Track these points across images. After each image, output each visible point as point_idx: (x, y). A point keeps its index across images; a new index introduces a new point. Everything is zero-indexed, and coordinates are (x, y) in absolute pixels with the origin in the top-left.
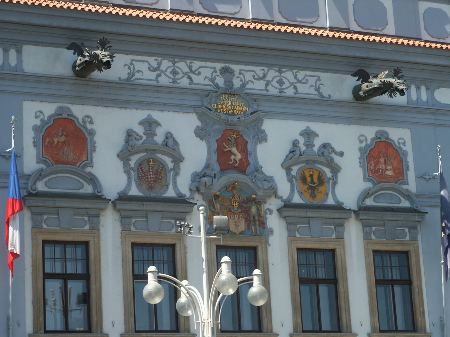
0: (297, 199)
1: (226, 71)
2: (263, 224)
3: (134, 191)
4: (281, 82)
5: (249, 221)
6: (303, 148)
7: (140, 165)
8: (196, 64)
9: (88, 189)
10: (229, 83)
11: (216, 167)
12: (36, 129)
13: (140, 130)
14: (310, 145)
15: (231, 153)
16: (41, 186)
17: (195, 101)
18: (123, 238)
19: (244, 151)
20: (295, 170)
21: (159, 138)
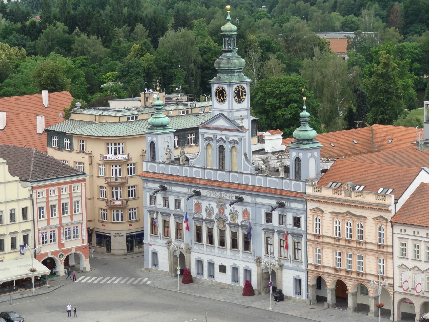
0: (231, 222)
1: (221, 194)
2: (226, 226)
3: (207, 218)
4: (229, 196)
5: (223, 225)
6: (232, 211)
7: (208, 212)
8: (216, 192)
9: (201, 217)
10: (221, 196)
11: (219, 214)
12: (194, 205)
13: (208, 206)
14: (234, 210)
15: (221, 211)
16: (195, 216)
17: (216, 200)
18: (206, 227)
19: (223, 211)
20: (231, 215)
21: (211, 208)
